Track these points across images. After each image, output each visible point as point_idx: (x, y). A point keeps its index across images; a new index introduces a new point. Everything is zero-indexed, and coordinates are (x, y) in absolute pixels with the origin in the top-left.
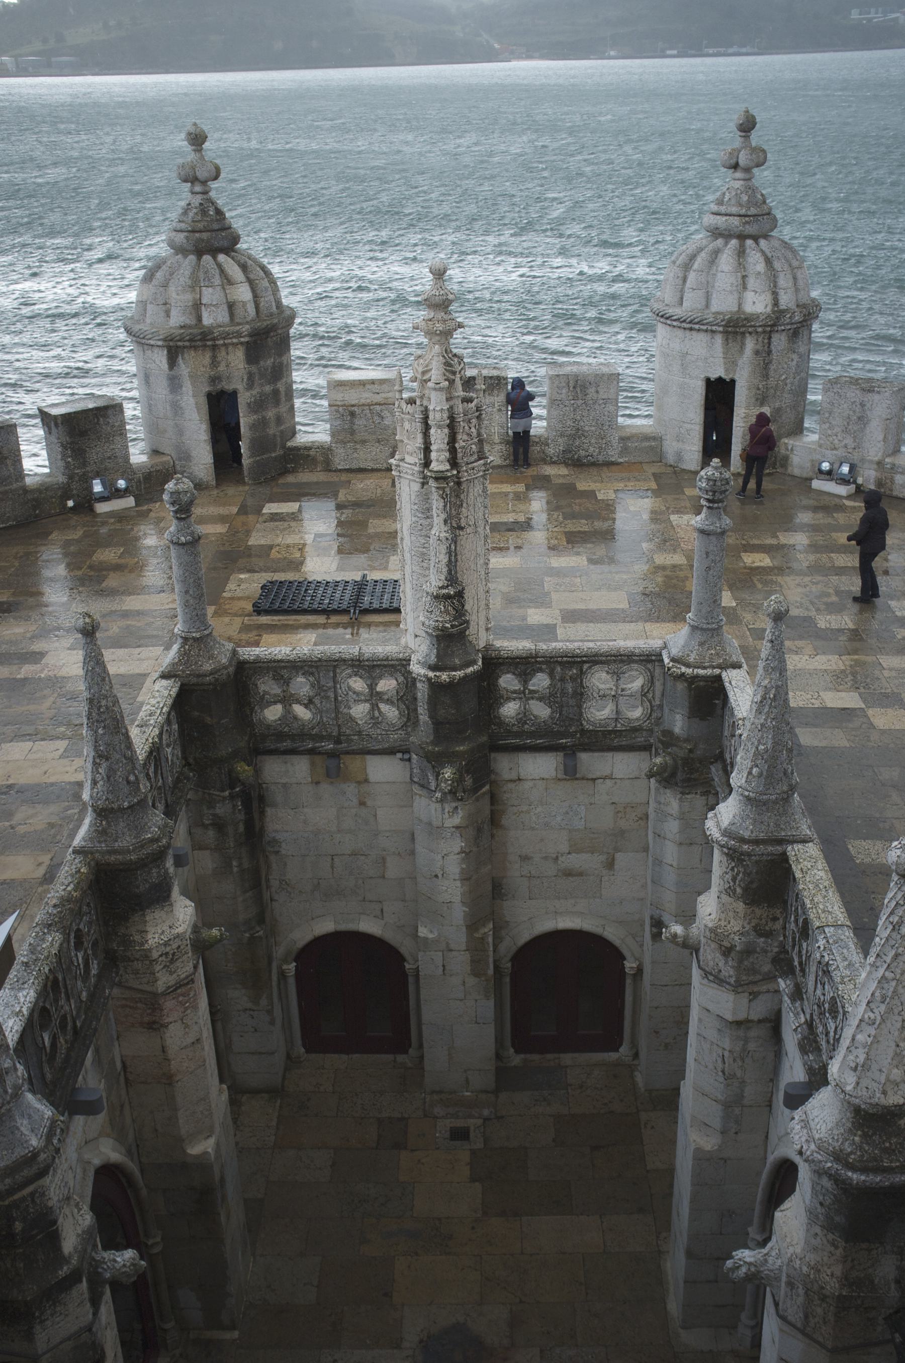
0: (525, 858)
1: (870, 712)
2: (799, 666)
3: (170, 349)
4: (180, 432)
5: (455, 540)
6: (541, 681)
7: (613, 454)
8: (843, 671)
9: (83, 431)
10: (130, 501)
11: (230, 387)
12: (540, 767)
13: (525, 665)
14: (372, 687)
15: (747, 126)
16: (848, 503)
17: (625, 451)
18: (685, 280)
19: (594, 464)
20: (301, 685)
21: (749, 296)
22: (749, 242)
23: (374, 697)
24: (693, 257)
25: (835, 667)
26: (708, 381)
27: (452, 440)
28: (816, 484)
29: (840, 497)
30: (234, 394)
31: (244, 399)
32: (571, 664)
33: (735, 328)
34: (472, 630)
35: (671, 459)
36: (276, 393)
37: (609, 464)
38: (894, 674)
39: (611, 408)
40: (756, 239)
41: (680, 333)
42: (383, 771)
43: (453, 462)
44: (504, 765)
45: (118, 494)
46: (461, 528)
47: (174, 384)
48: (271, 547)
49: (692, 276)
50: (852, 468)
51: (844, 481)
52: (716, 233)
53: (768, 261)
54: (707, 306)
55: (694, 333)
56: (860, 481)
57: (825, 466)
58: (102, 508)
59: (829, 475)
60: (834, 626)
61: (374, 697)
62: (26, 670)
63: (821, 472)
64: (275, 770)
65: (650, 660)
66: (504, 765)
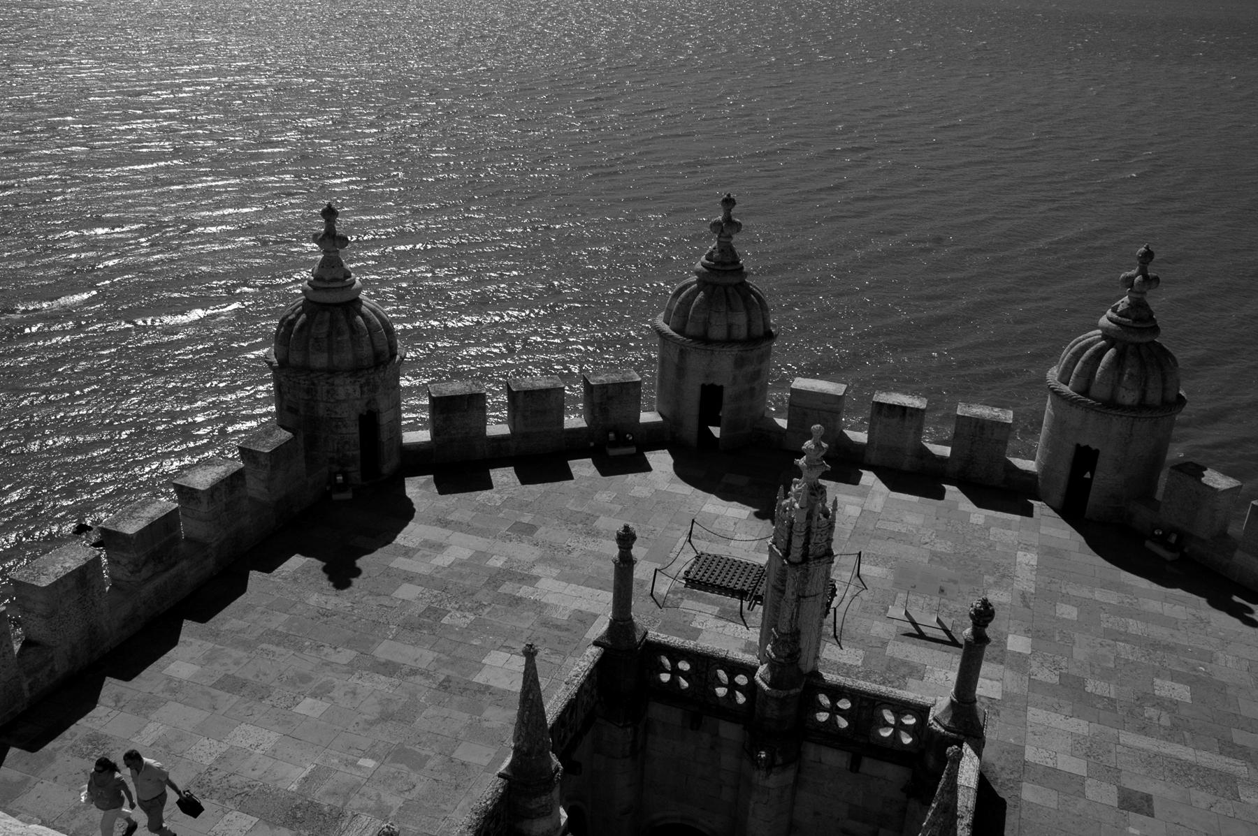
0: (816, 814)
3: (681, 351)
5: (798, 607)
6: (845, 704)
8: (1085, 738)
9: (609, 400)
11: (718, 384)
12: (834, 759)
13: (836, 692)
14: (731, 678)
20: (684, 666)
21: (1122, 392)
23: (732, 686)
25: (1080, 732)
27: (807, 542)
28: (1148, 544)
30: (721, 389)
31: (728, 393)
32: (867, 699)
34: (803, 660)
36: (752, 389)
42: (730, 732)
43: (805, 558)
44: (811, 751)
46: (804, 597)
47: (681, 371)
48: (717, 517)
56: (1186, 550)
58: (613, 452)
59: (1162, 541)
60: (1099, 692)
61: (732, 686)
62: (524, 591)
64: (657, 711)
65: (922, 711)
66: (811, 751)
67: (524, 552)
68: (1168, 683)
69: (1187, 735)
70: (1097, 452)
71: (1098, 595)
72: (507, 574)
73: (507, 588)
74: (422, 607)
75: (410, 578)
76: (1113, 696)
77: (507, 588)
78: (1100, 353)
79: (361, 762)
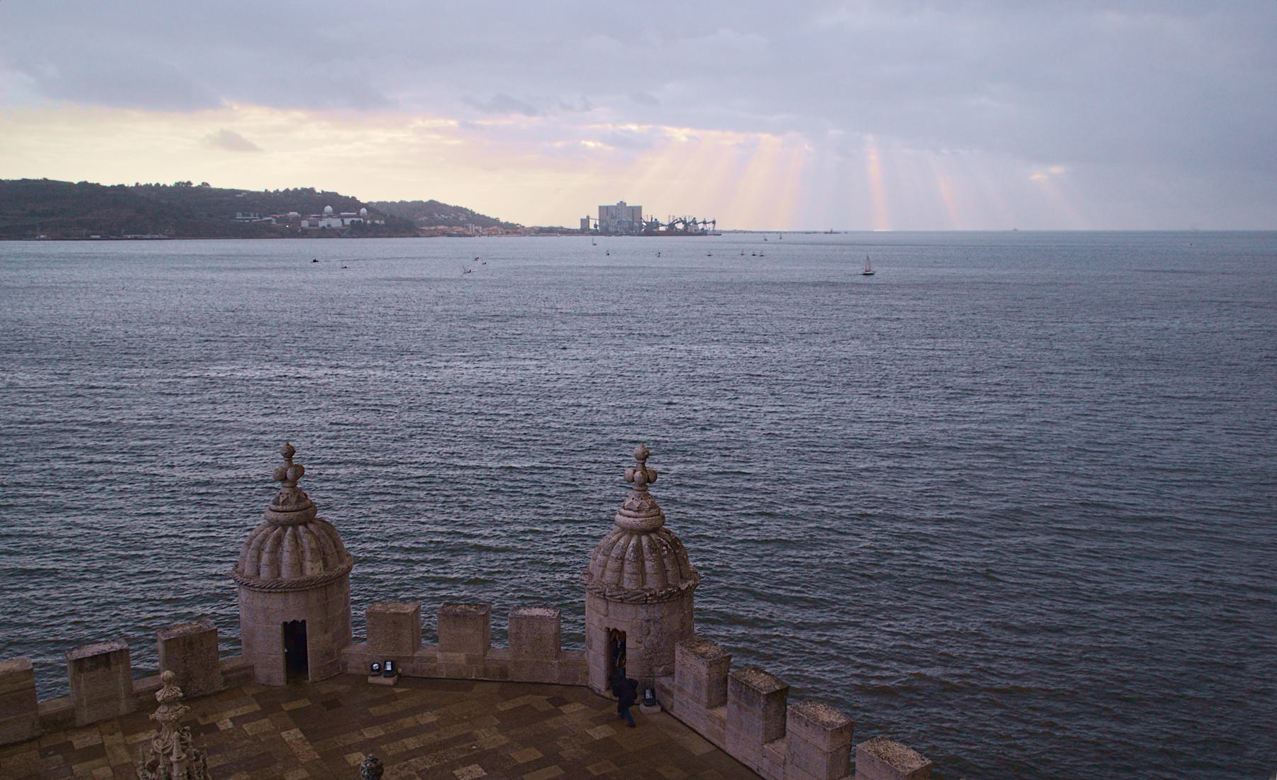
15: (289, 453)
16: (398, 690)
18: (259, 558)
19: (204, 696)
21: (308, 565)
22: (301, 528)
24: (263, 542)
26: (285, 624)
28: (371, 679)
29: (389, 686)
33: (301, 587)
35: (263, 680)
40: (305, 524)
41: (261, 595)
49: (265, 557)
52: (274, 524)
53: (317, 539)
54: (279, 575)
55: (273, 596)
59: (381, 671)
70: (304, 622)
71: (368, 734)
78: (279, 541)
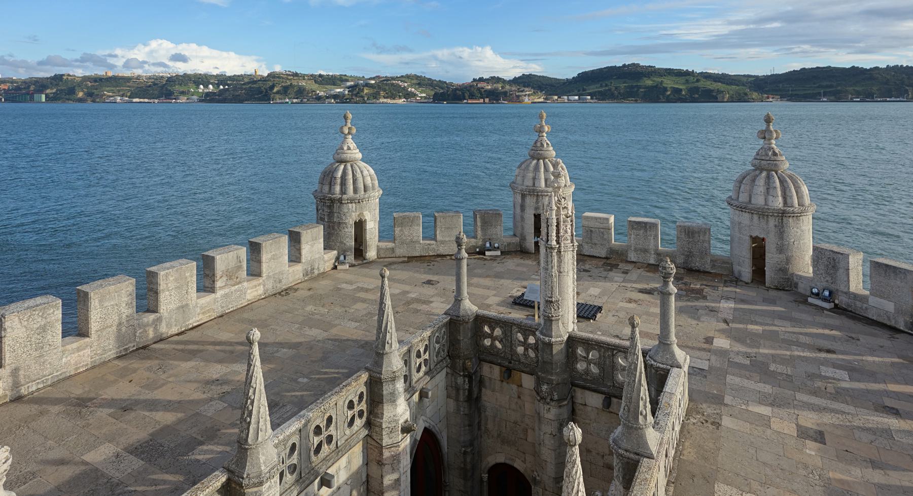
1: (773, 420)
2: (746, 385)
4: (523, 228)
7: (708, 268)
8: (769, 394)
10: (499, 253)
17: (713, 266)
28: (810, 300)
35: (736, 274)
37: (705, 272)
38: (801, 404)
39: (706, 245)
42: (528, 381)
45: (496, 249)
50: (831, 293)
51: (825, 300)
56: (837, 302)
57: (815, 291)
58: (487, 253)
59: (817, 295)
60: (779, 371)
62: (424, 307)
63: (812, 293)
67: (428, 291)
68: (831, 369)
69: (848, 399)
72: (417, 301)
73: (414, 306)
74: (365, 312)
75: (364, 301)
76: (789, 373)
77: (414, 306)
79: (300, 380)
